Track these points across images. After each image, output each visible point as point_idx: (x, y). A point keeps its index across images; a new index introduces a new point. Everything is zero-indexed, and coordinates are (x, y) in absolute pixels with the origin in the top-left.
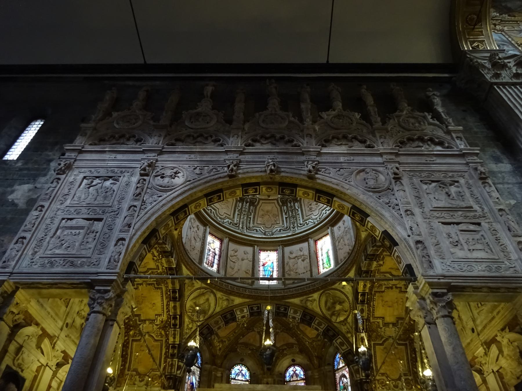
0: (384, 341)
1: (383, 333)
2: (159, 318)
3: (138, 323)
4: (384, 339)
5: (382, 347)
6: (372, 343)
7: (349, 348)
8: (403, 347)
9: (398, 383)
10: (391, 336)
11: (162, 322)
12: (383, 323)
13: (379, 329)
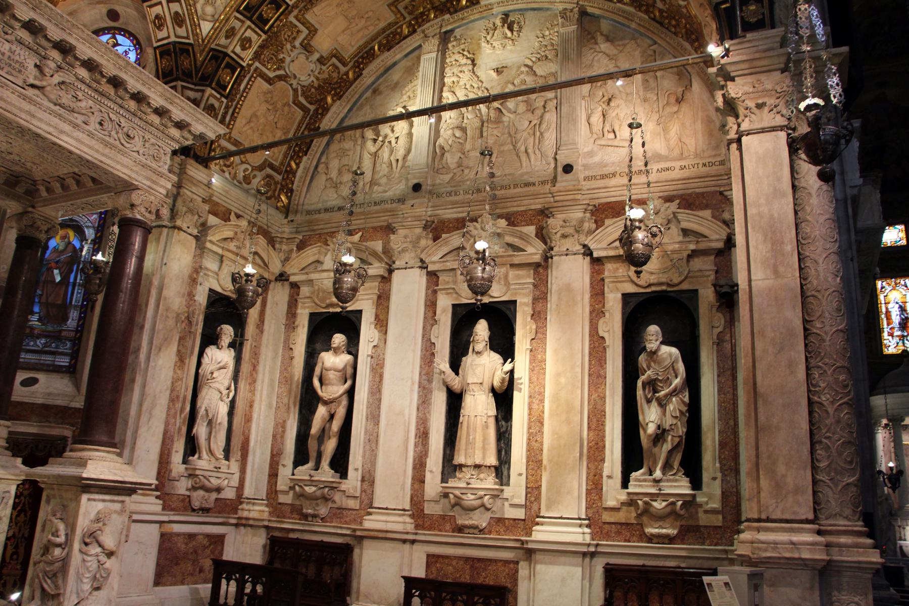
0: (280, 78)
1: (288, 59)
4: (281, 72)
5: (266, 86)
6: (257, 64)
7: (191, 41)
8: (299, 113)
9: (255, 177)
10: (298, 76)
12: (305, 39)
13: (288, 46)
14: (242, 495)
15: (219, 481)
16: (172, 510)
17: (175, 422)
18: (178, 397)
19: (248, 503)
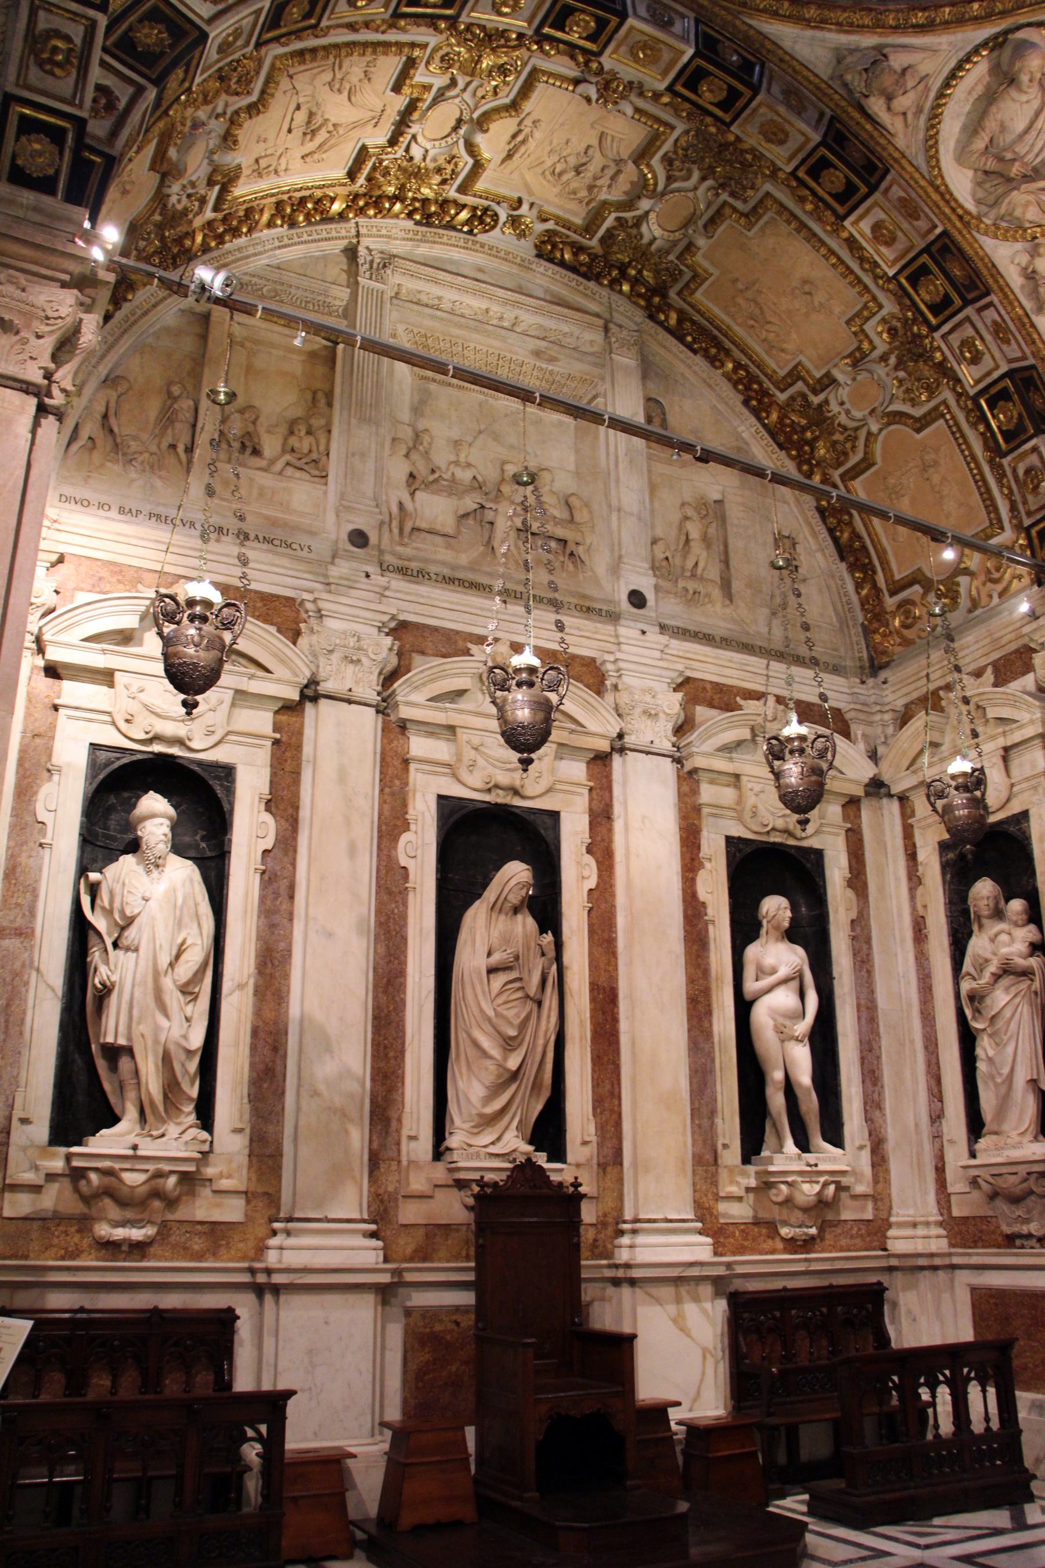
2: (868, 327)
3: (816, 400)
11: (892, 331)
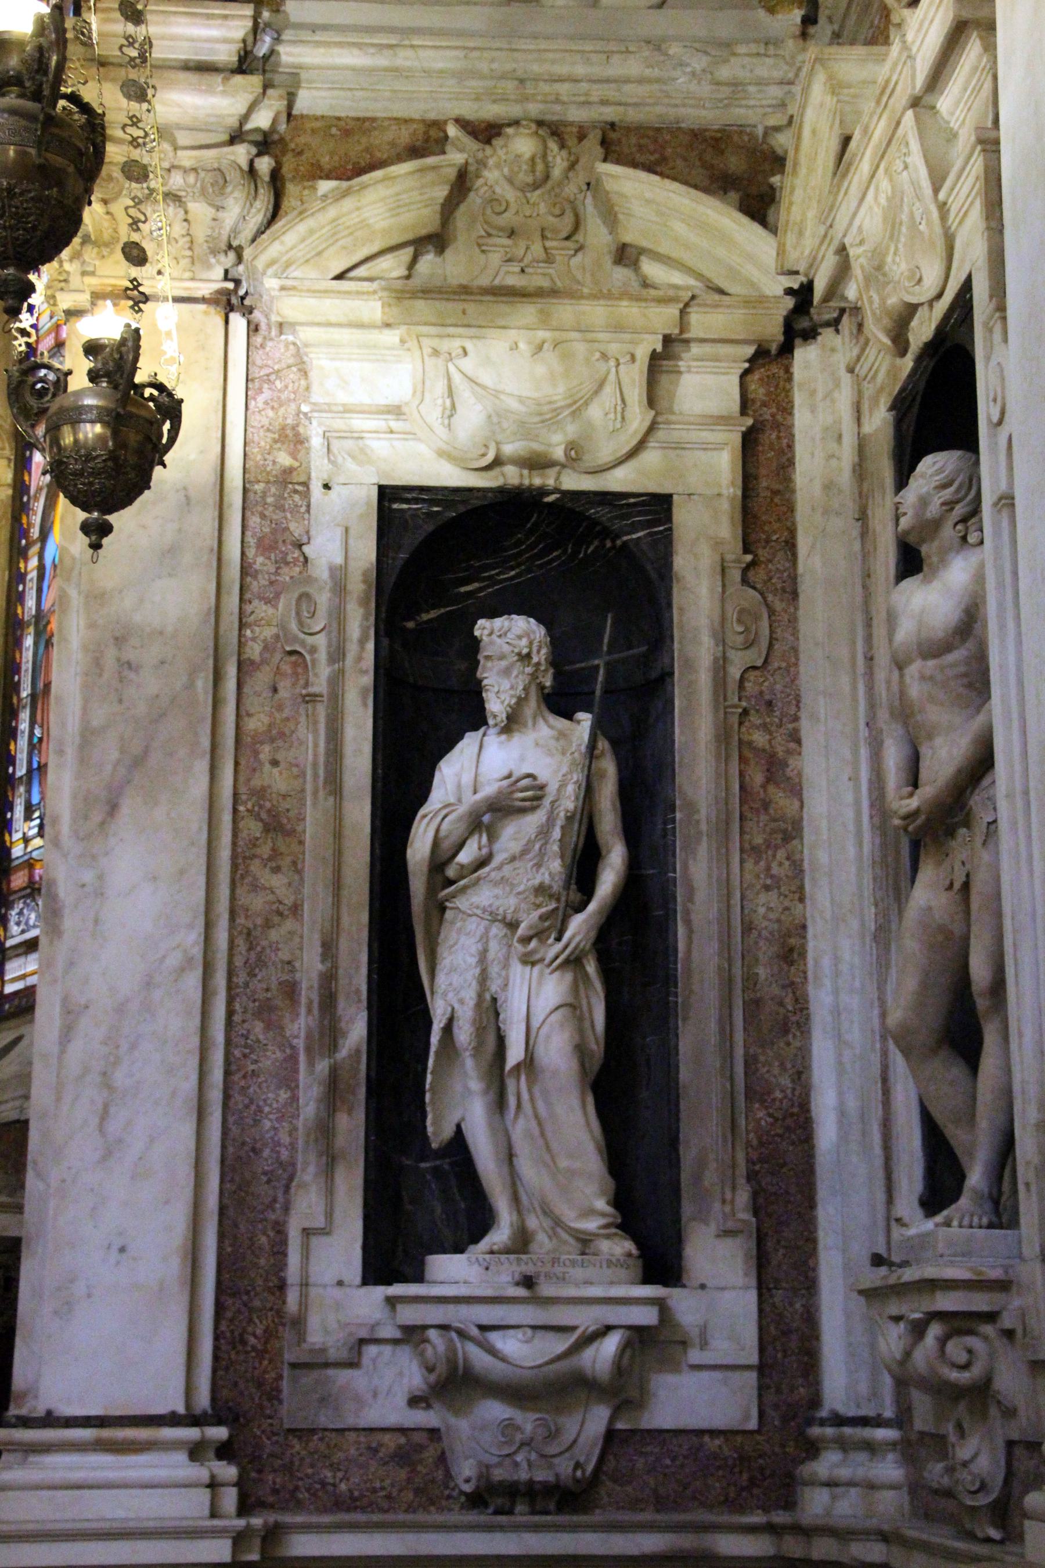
14: (815, 1402)
15: (560, 1344)
16: (339, 1504)
17: (294, 1098)
18: (290, 990)
19: (844, 1445)
